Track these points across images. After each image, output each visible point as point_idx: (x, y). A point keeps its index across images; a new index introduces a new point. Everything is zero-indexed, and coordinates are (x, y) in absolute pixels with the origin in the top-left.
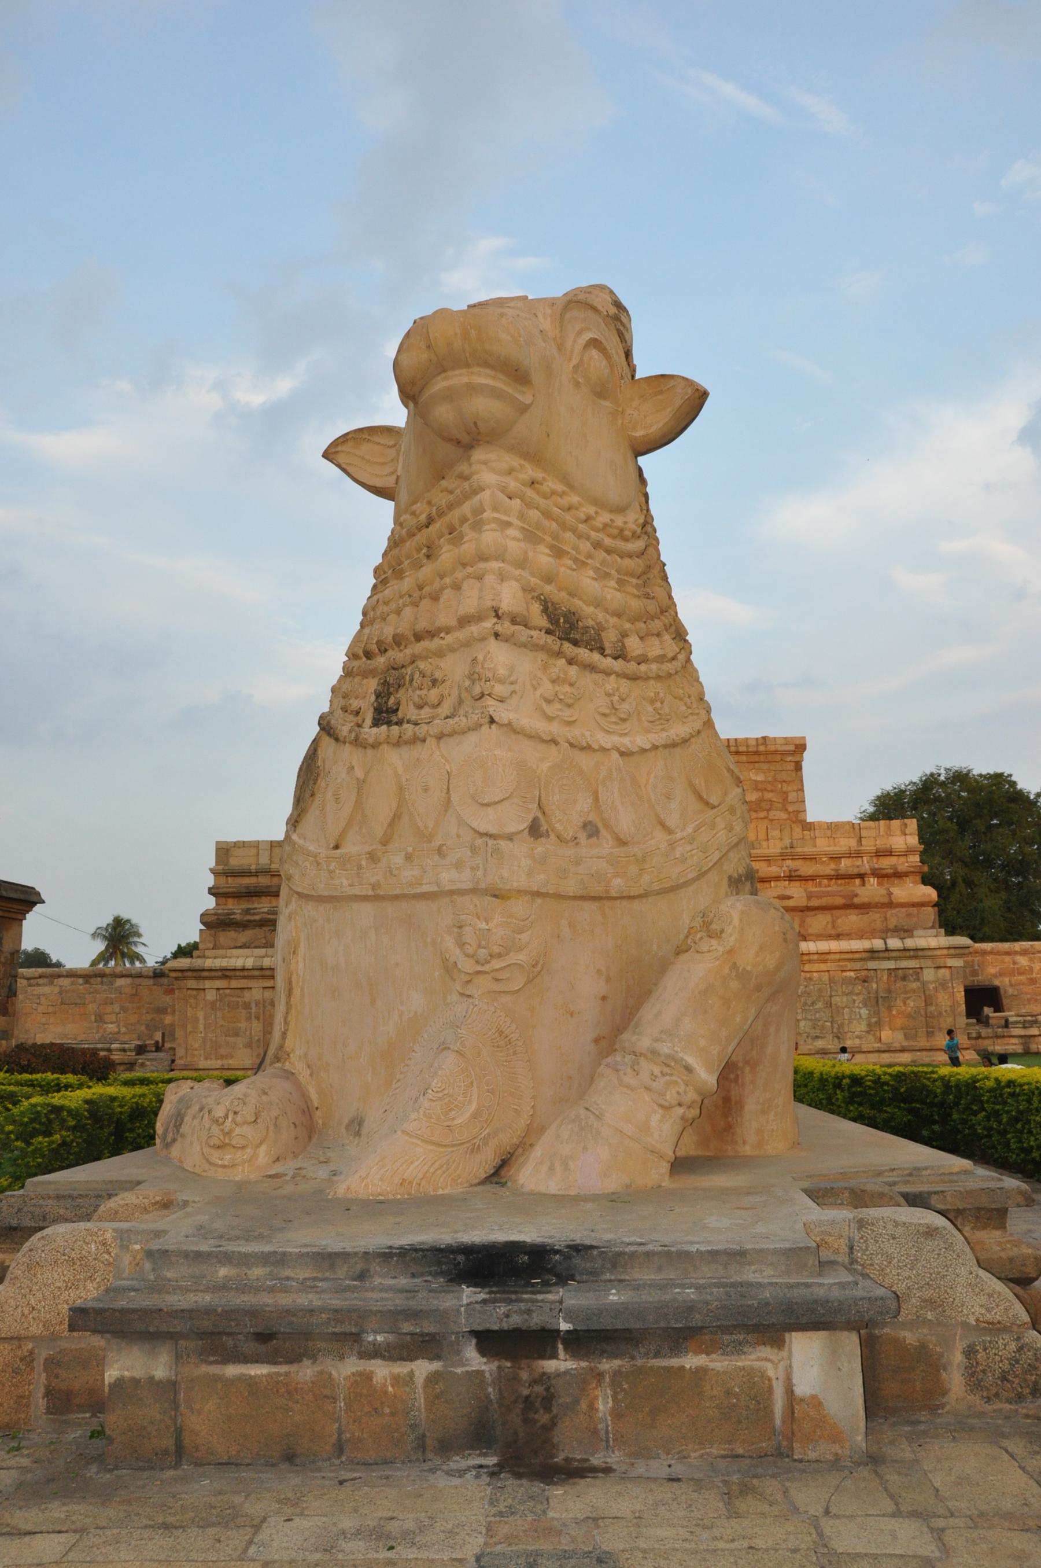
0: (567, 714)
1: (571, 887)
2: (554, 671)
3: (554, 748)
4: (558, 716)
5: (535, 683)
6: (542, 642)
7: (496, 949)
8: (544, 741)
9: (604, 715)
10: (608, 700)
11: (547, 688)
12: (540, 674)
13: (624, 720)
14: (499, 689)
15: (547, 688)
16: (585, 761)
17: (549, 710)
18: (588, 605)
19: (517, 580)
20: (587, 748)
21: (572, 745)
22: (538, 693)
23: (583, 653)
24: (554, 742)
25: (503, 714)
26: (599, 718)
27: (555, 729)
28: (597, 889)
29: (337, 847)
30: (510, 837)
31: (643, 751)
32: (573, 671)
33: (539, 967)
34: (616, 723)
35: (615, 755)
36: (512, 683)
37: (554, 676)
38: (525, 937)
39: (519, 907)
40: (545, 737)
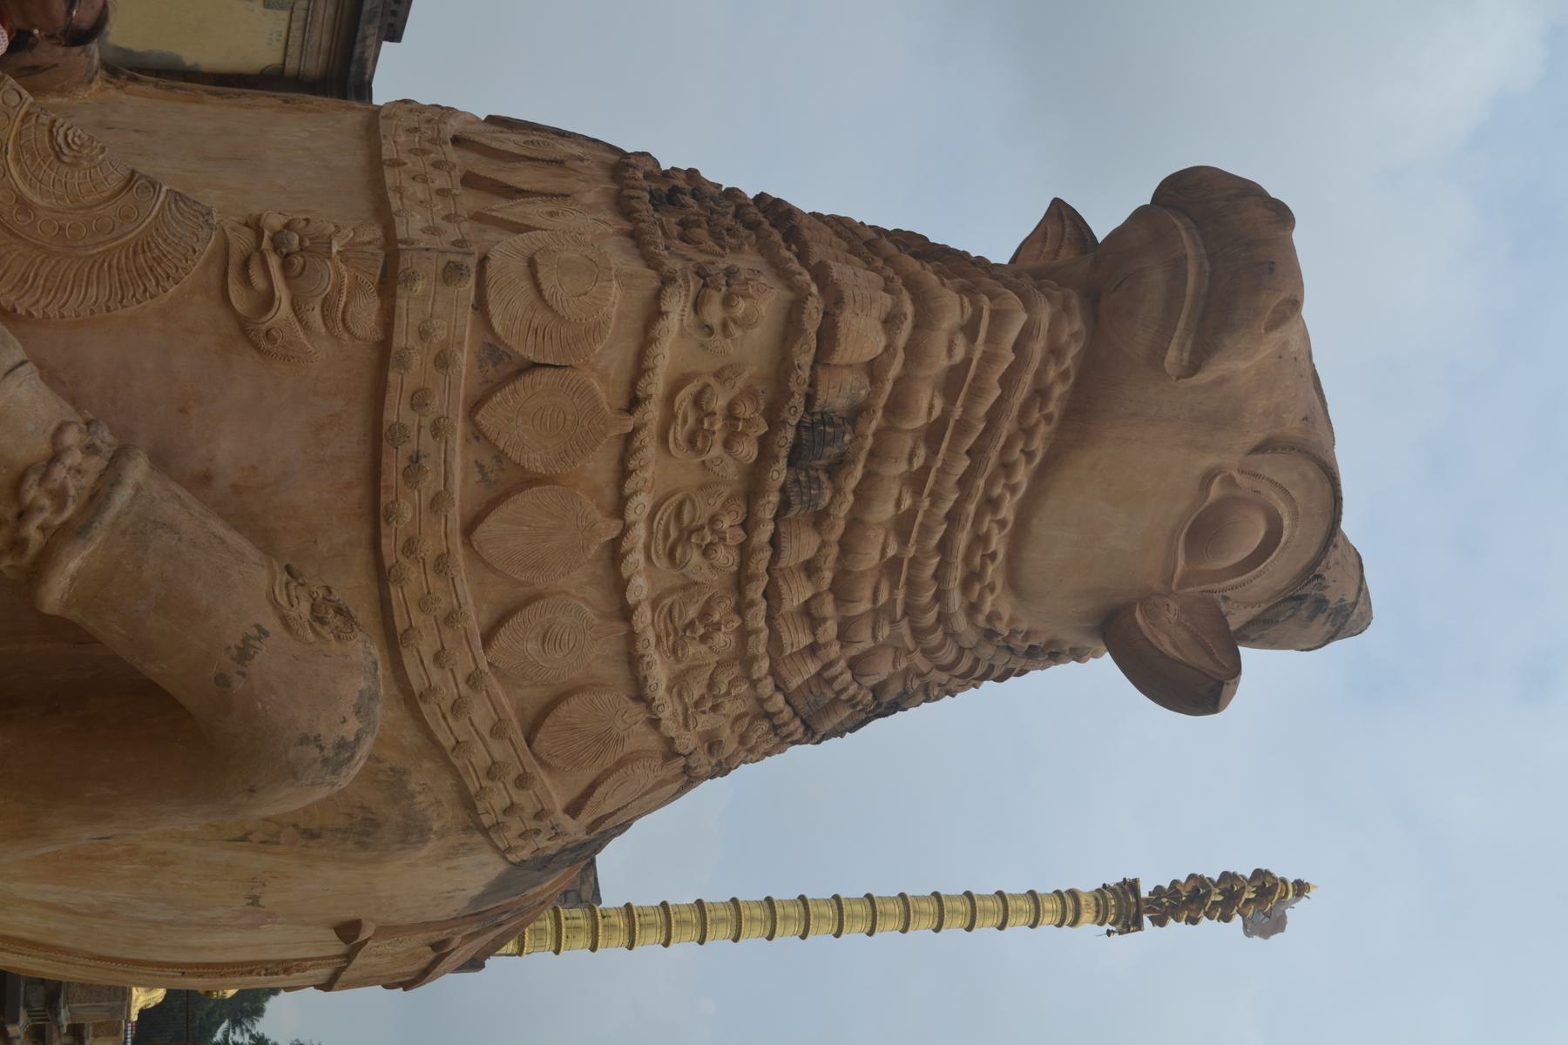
0: (679, 433)
1: (396, 411)
2: (746, 410)
3: (622, 402)
4: (675, 417)
5: (727, 373)
6: (793, 387)
7: (298, 261)
8: (633, 384)
9: (679, 512)
10: (704, 520)
12: (740, 383)
13: (671, 554)
16: (599, 465)
17: (685, 395)
19: (887, 348)
20: (624, 473)
21: (629, 438)
22: (712, 381)
23: (779, 474)
24: (634, 402)
25: (677, 308)
27: (652, 412)
28: (392, 474)
30: (481, 305)
31: (621, 585)
32: (748, 450)
33: (264, 344)
34: (667, 535)
35: (611, 529)
36: (725, 326)
38: (316, 317)
39: (366, 313)
40: (642, 383)
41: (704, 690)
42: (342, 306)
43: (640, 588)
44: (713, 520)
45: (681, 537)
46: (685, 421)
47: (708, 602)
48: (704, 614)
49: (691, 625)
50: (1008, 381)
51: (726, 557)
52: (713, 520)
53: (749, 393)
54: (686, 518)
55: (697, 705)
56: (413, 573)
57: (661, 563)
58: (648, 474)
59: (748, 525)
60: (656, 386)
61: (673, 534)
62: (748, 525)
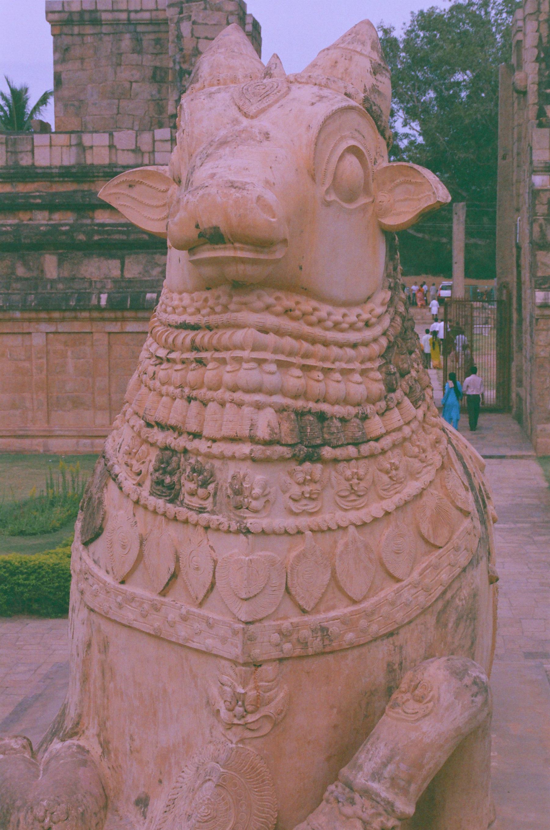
0: (311, 506)
4: (304, 510)
10: (347, 484)
11: (296, 490)
12: (289, 480)
14: (254, 504)
15: (296, 490)
17: (296, 508)
18: (333, 405)
22: (288, 495)
24: (300, 532)
26: (338, 499)
27: (303, 522)
29: (123, 582)
33: (283, 715)
35: (352, 529)
37: (301, 480)
41: (417, 460)
42: (267, 684)
43: (376, 509)
44: (348, 480)
45: (354, 494)
46: (306, 505)
47: (381, 470)
48: (387, 472)
49: (391, 478)
50: (279, 332)
51: (361, 468)
52: (348, 480)
53: (291, 474)
54: (347, 493)
55: (422, 461)
56: (374, 628)
57: (363, 500)
58: (327, 517)
59: (348, 460)
60: (291, 523)
61: (353, 497)
62: (348, 460)
